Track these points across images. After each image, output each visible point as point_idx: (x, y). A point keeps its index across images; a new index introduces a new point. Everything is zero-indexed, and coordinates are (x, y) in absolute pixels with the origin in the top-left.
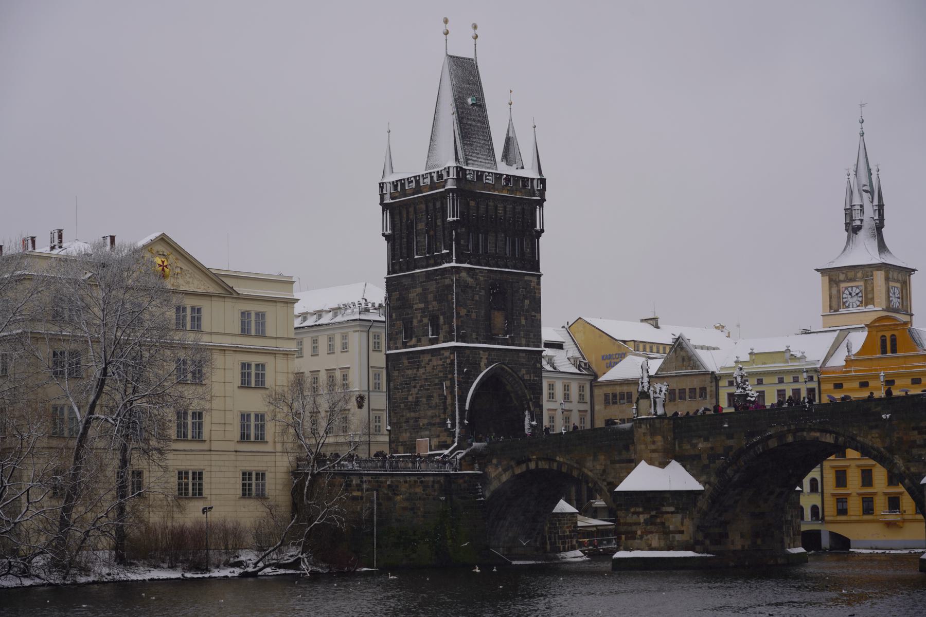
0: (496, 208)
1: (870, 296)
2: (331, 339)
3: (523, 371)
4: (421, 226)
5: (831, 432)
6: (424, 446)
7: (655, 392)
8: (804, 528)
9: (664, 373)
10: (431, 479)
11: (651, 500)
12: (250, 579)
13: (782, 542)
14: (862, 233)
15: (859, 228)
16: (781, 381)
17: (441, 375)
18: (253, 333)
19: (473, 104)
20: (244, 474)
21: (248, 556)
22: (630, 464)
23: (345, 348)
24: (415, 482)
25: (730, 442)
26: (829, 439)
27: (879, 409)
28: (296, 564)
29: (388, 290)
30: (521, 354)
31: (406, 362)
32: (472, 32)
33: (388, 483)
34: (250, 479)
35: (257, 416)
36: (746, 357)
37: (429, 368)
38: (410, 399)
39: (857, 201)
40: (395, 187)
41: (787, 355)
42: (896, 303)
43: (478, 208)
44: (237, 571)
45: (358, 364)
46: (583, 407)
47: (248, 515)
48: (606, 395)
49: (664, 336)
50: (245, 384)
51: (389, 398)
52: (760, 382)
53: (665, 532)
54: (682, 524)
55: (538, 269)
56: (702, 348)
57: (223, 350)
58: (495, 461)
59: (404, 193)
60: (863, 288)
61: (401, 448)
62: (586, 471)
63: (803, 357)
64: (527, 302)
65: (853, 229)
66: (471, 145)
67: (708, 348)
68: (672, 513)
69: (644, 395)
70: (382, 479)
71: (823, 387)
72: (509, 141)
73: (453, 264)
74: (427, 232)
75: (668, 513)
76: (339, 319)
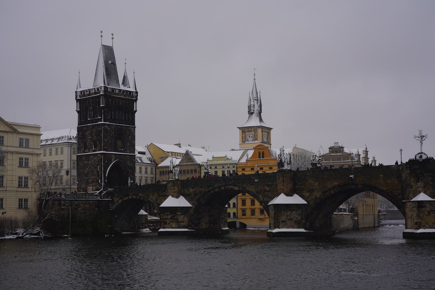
1: (256, 137)
2: (57, 149)
3: (128, 162)
4: (91, 108)
5: (237, 186)
6: (90, 190)
7: (175, 171)
8: (229, 220)
9: (182, 164)
10: (92, 202)
12: (20, 240)
13: (220, 225)
14: (254, 115)
15: (253, 113)
16: (223, 167)
17: (97, 163)
18: (24, 146)
20: (19, 200)
21: (20, 231)
22: (165, 197)
23: (62, 152)
24: (86, 203)
25: (202, 189)
26: (236, 188)
27: (254, 178)
28: (38, 234)
29: (78, 132)
31: (84, 158)
32: (111, 37)
34: (22, 202)
35: (25, 178)
36: (211, 159)
37: (93, 161)
38: (85, 172)
39: (252, 103)
40: (81, 93)
41: (226, 158)
42: (265, 140)
44: (15, 236)
45: (66, 159)
46: (152, 176)
47: (21, 215)
48: (161, 172)
49: (183, 150)
50: (21, 166)
51: (78, 172)
52: (216, 168)
53: (178, 222)
55: (134, 125)
56: (196, 155)
57: (12, 153)
58: (116, 195)
59: (84, 95)
61: (81, 190)
62: (149, 199)
63: (231, 159)
64: (130, 137)
65: (251, 113)
67: (198, 155)
68: (180, 215)
69: (171, 172)
70: (74, 202)
71: (238, 170)
72: (125, 78)
73: (102, 122)
74: (93, 110)
75: (179, 215)
76: (60, 142)
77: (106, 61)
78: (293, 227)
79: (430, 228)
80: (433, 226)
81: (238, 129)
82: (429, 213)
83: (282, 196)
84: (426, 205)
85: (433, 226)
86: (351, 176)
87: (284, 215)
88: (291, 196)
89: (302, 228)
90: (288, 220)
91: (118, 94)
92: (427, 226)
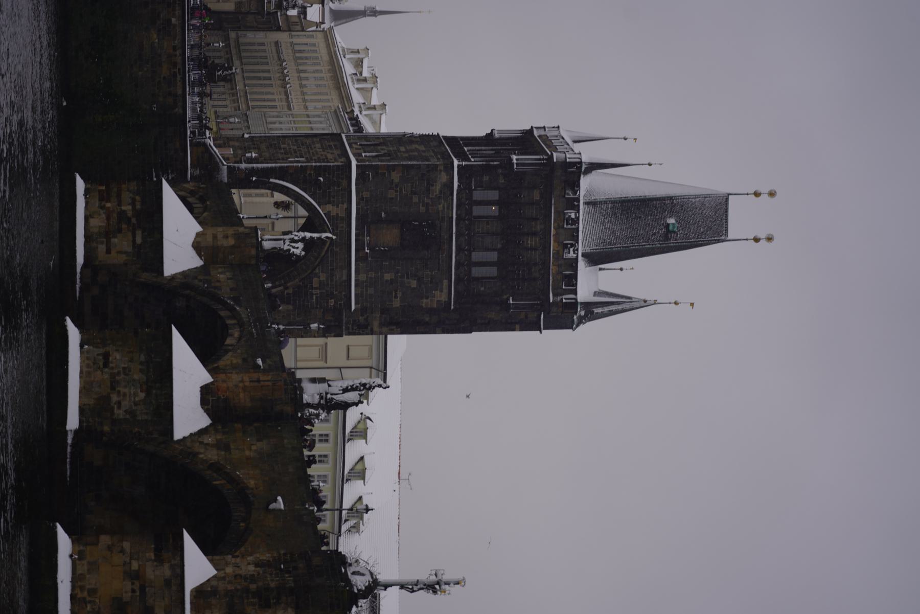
0: (535, 234)
3: (323, 277)
10: (180, 92)
19: (668, 225)
24: (175, 64)
30: (345, 272)
33: (173, 20)
53: (108, 234)
54: (119, 252)
64: (414, 284)
66: (614, 214)
68: (134, 241)
70: (178, 12)
73: (456, 163)
75: (134, 236)
77: (674, 205)
78: (84, 390)
79: (76, 579)
80: (82, 588)
82: (135, 576)
83: (204, 377)
84: (166, 566)
85: (82, 588)
86: (279, 498)
87: (131, 360)
88: (204, 402)
89: (81, 422)
90: (113, 376)
91: (559, 227)
92: (83, 568)
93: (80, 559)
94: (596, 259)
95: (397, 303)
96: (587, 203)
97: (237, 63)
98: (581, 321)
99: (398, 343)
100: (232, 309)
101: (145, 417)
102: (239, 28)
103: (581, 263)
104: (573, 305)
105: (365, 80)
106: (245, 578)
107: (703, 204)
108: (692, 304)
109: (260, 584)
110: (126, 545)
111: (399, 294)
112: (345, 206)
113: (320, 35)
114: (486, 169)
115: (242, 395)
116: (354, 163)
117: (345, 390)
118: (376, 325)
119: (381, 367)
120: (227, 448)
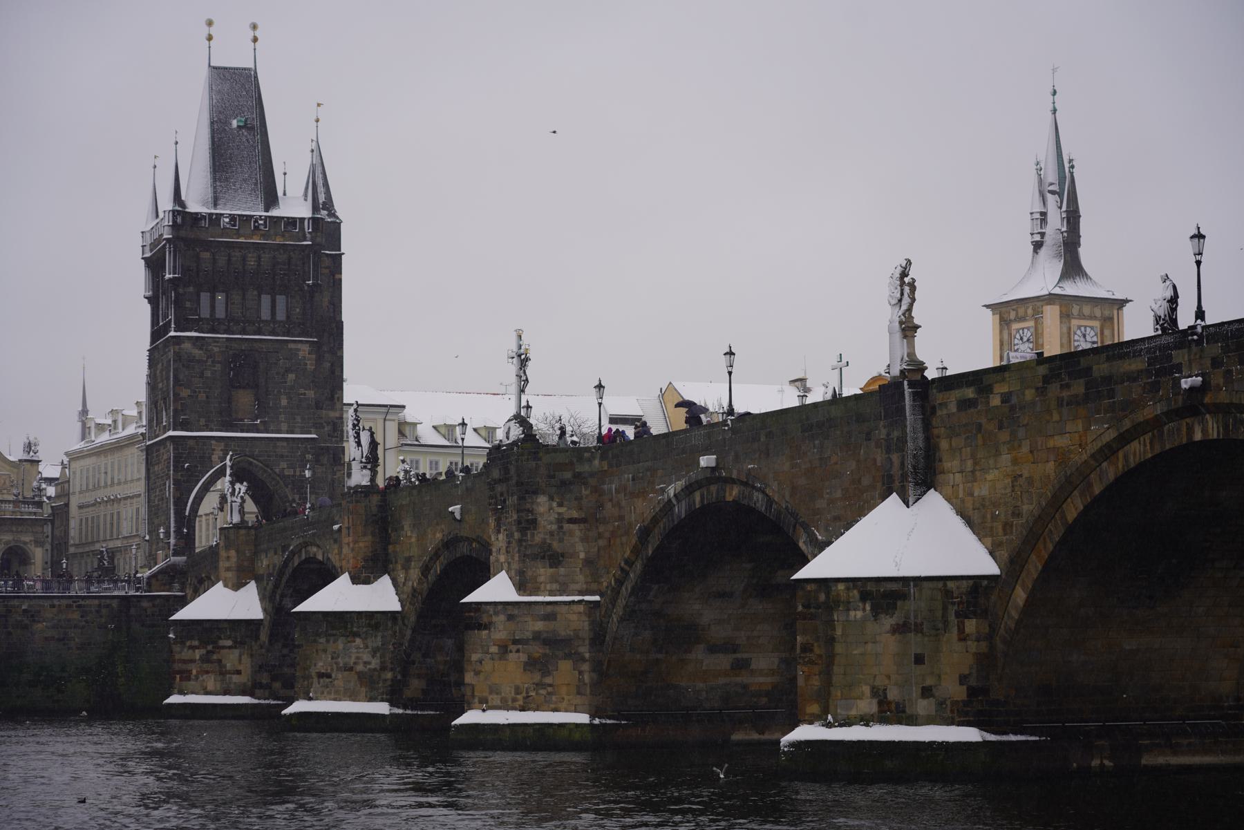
0: (244, 259)
3: (284, 465)
10: (96, 602)
11: (209, 630)
14: (1043, 251)
19: (239, 127)
24: (69, 606)
30: (279, 444)
33: (24, 607)
43: (214, 261)
53: (223, 673)
54: (240, 660)
60: (1032, 330)
64: (291, 376)
65: (1037, 246)
68: (230, 648)
70: (16, 602)
73: (172, 334)
75: (224, 647)
78: (354, 697)
80: (514, 700)
81: (989, 312)
82: (504, 649)
83: (344, 580)
84: (495, 619)
85: (514, 700)
87: (325, 651)
88: (367, 582)
89: (382, 700)
90: (339, 669)
92: (496, 700)
93: (487, 702)
94: (271, 199)
95: (311, 394)
96: (215, 205)
97: (97, 546)
98: (332, 214)
99: (352, 392)
100: (293, 553)
101: (379, 638)
102: (66, 543)
103: (274, 213)
104: (315, 221)
105: (115, 422)
106: (509, 543)
107: (219, 92)
108: (319, 105)
109: (514, 528)
110: (475, 657)
111: (302, 391)
112: (213, 442)
113: (73, 465)
114: (178, 303)
115: (361, 545)
116: (171, 433)
117: (359, 444)
118: (333, 414)
119: (384, 410)
120: (409, 560)
